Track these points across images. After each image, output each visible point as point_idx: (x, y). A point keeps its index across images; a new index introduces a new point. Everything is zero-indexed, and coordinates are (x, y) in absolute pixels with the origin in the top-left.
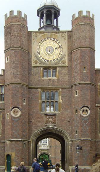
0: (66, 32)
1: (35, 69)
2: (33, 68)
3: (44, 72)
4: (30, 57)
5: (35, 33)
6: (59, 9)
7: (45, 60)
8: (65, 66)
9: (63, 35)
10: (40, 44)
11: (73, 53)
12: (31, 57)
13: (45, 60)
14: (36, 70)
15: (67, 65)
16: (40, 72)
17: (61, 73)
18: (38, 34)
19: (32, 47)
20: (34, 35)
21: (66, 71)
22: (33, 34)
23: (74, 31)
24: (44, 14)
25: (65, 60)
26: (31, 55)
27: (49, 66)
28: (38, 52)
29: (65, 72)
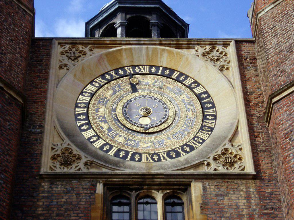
0: (226, 44)
1: (59, 188)
2: (46, 185)
3: (115, 208)
4: (31, 133)
5: (67, 47)
6: (182, 21)
7: (122, 154)
8: (243, 177)
9: (214, 54)
10: (91, 88)
11: (277, 106)
12: (42, 133)
13: (122, 154)
14: (68, 192)
15: (250, 169)
16: (91, 203)
17: (221, 210)
18: (87, 50)
19: (50, 96)
20: (62, 54)
21: (248, 198)
22: (57, 50)
23: (267, 24)
24: (115, 30)
25: (234, 150)
26: (42, 127)
27: (143, 176)
28: (82, 117)
29: (242, 203)
